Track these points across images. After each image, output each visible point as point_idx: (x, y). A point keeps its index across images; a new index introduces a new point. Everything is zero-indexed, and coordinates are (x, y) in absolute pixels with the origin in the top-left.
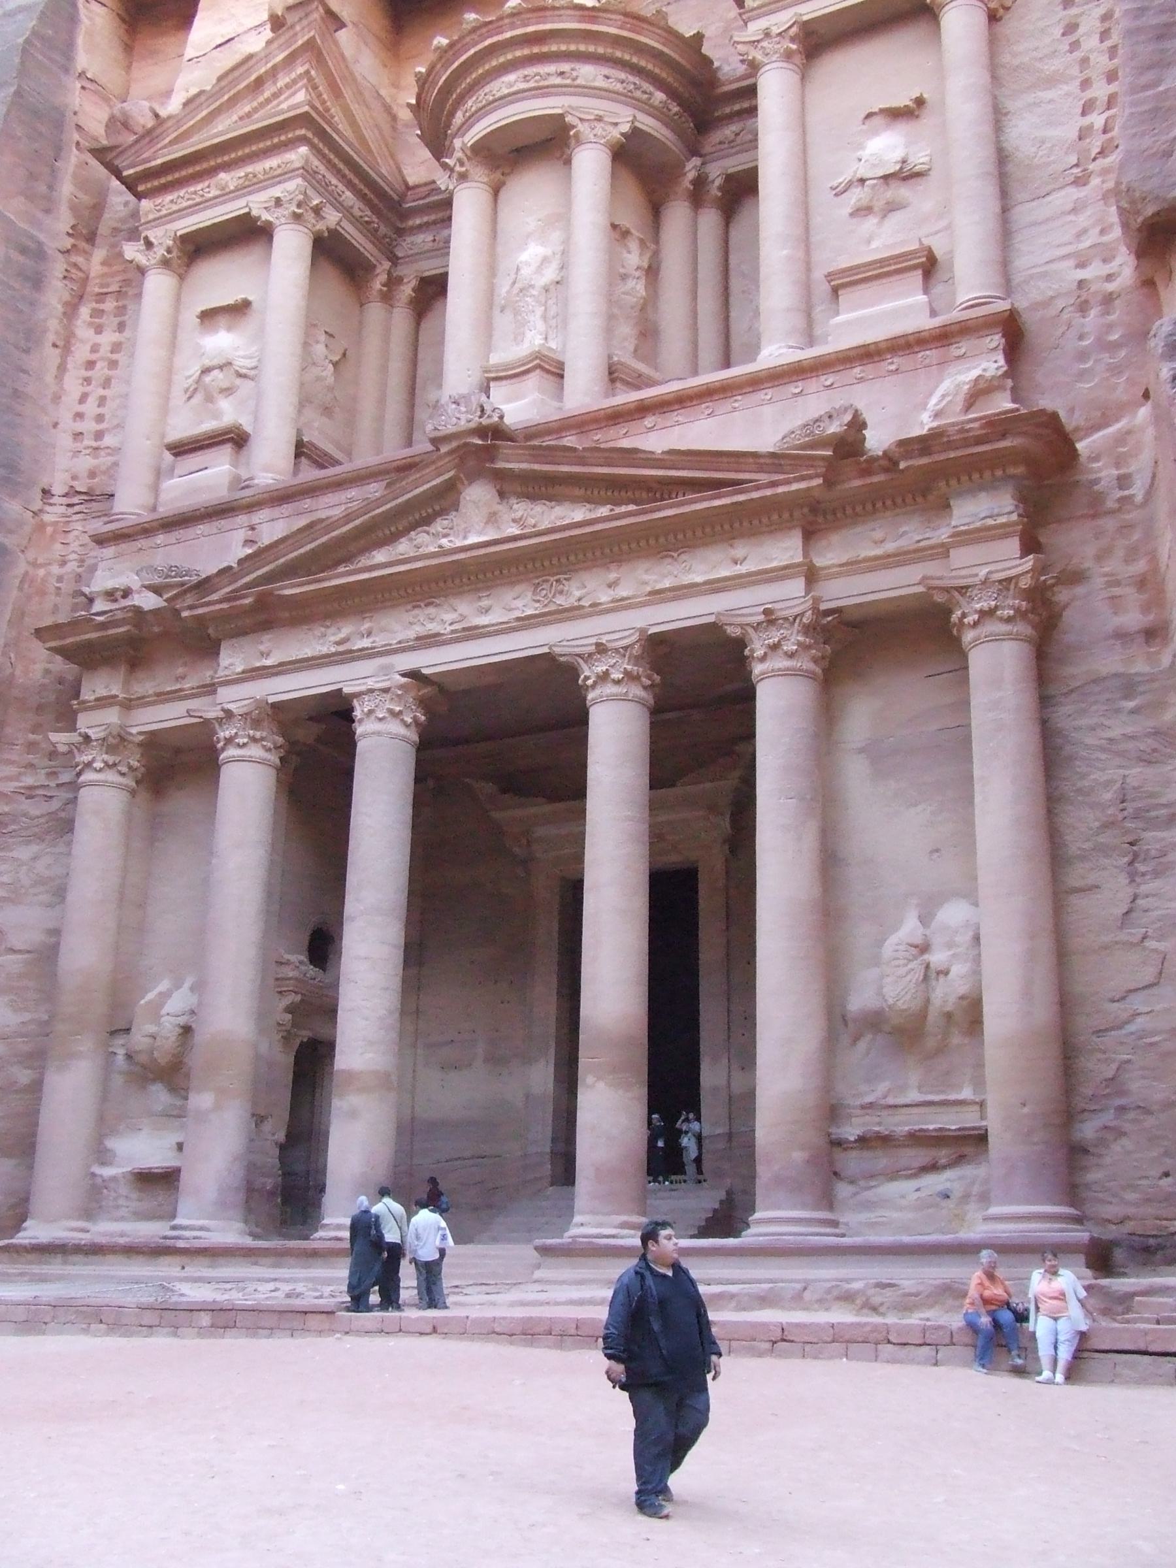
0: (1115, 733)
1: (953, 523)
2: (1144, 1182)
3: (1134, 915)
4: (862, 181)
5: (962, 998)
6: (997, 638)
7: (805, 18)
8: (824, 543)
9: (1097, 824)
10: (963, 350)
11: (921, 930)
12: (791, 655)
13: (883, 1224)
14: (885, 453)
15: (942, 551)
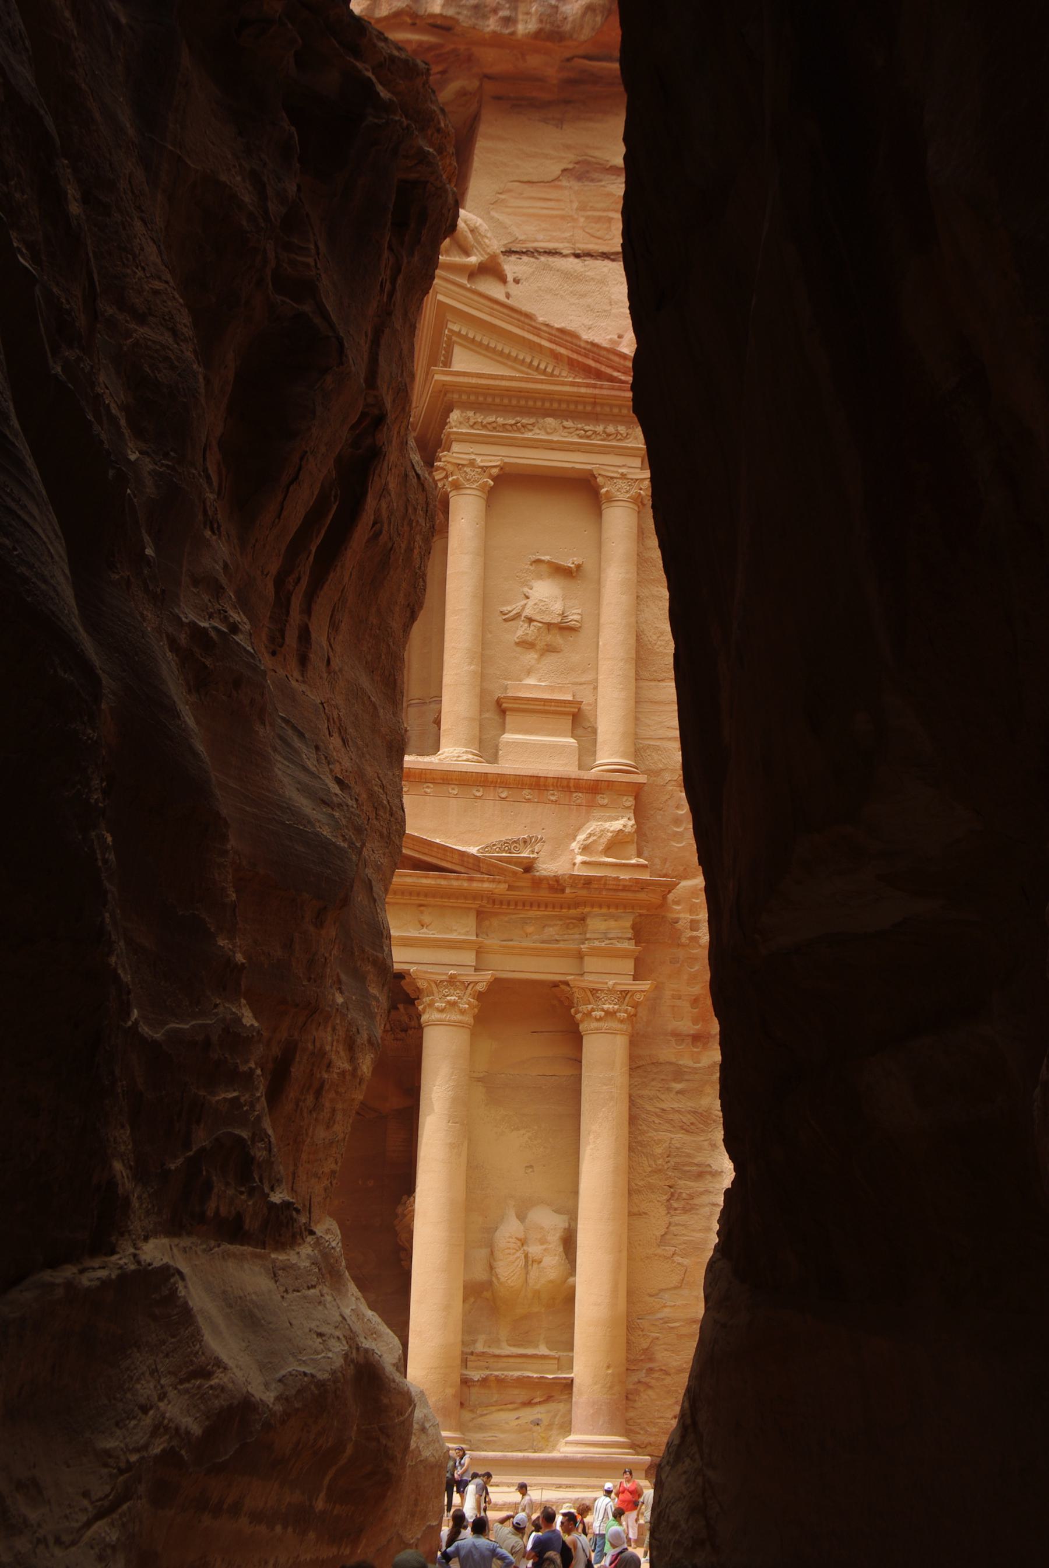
0: (664, 1106)
1: (588, 936)
2: (662, 1421)
3: (667, 1237)
4: (530, 620)
5: (551, 1281)
6: (613, 1033)
7: (506, 460)
8: (487, 923)
9: (650, 1169)
10: (605, 801)
11: (522, 1228)
12: (463, 1012)
13: (494, 1441)
14: (556, 879)
15: (580, 956)
